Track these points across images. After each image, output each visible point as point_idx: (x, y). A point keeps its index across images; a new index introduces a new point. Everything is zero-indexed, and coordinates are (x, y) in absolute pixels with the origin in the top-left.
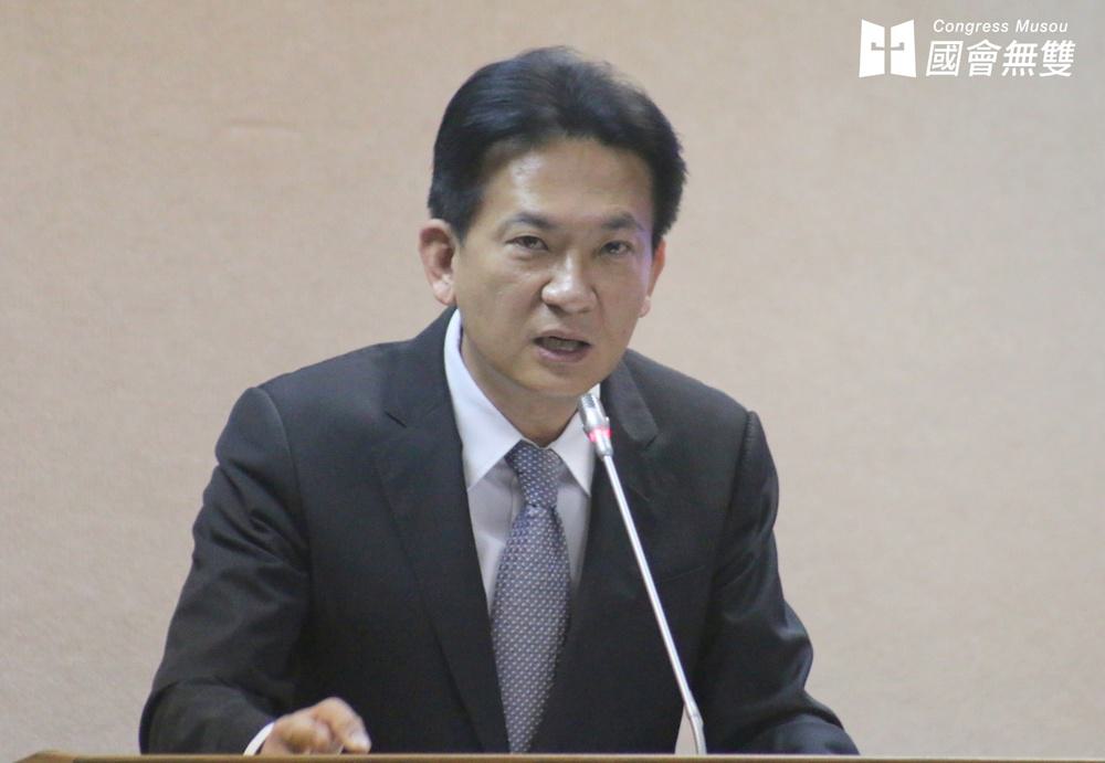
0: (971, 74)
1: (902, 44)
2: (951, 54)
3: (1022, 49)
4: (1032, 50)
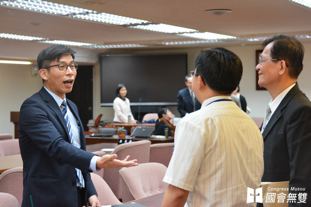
0: (278, 202)
1: (259, 194)
2: (272, 197)
3: (292, 195)
4: (295, 196)
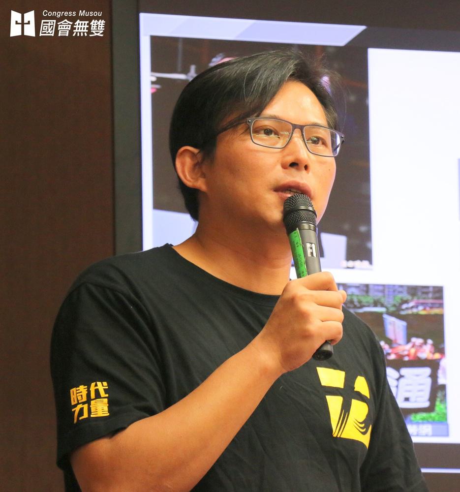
0: (59, 35)
1: (29, 22)
2: (51, 26)
3: (82, 23)
4: (86, 24)
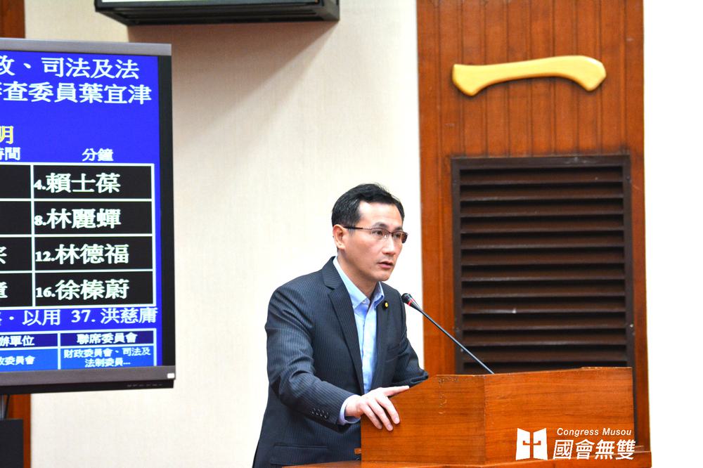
2: (567, 447)
4: (611, 445)
